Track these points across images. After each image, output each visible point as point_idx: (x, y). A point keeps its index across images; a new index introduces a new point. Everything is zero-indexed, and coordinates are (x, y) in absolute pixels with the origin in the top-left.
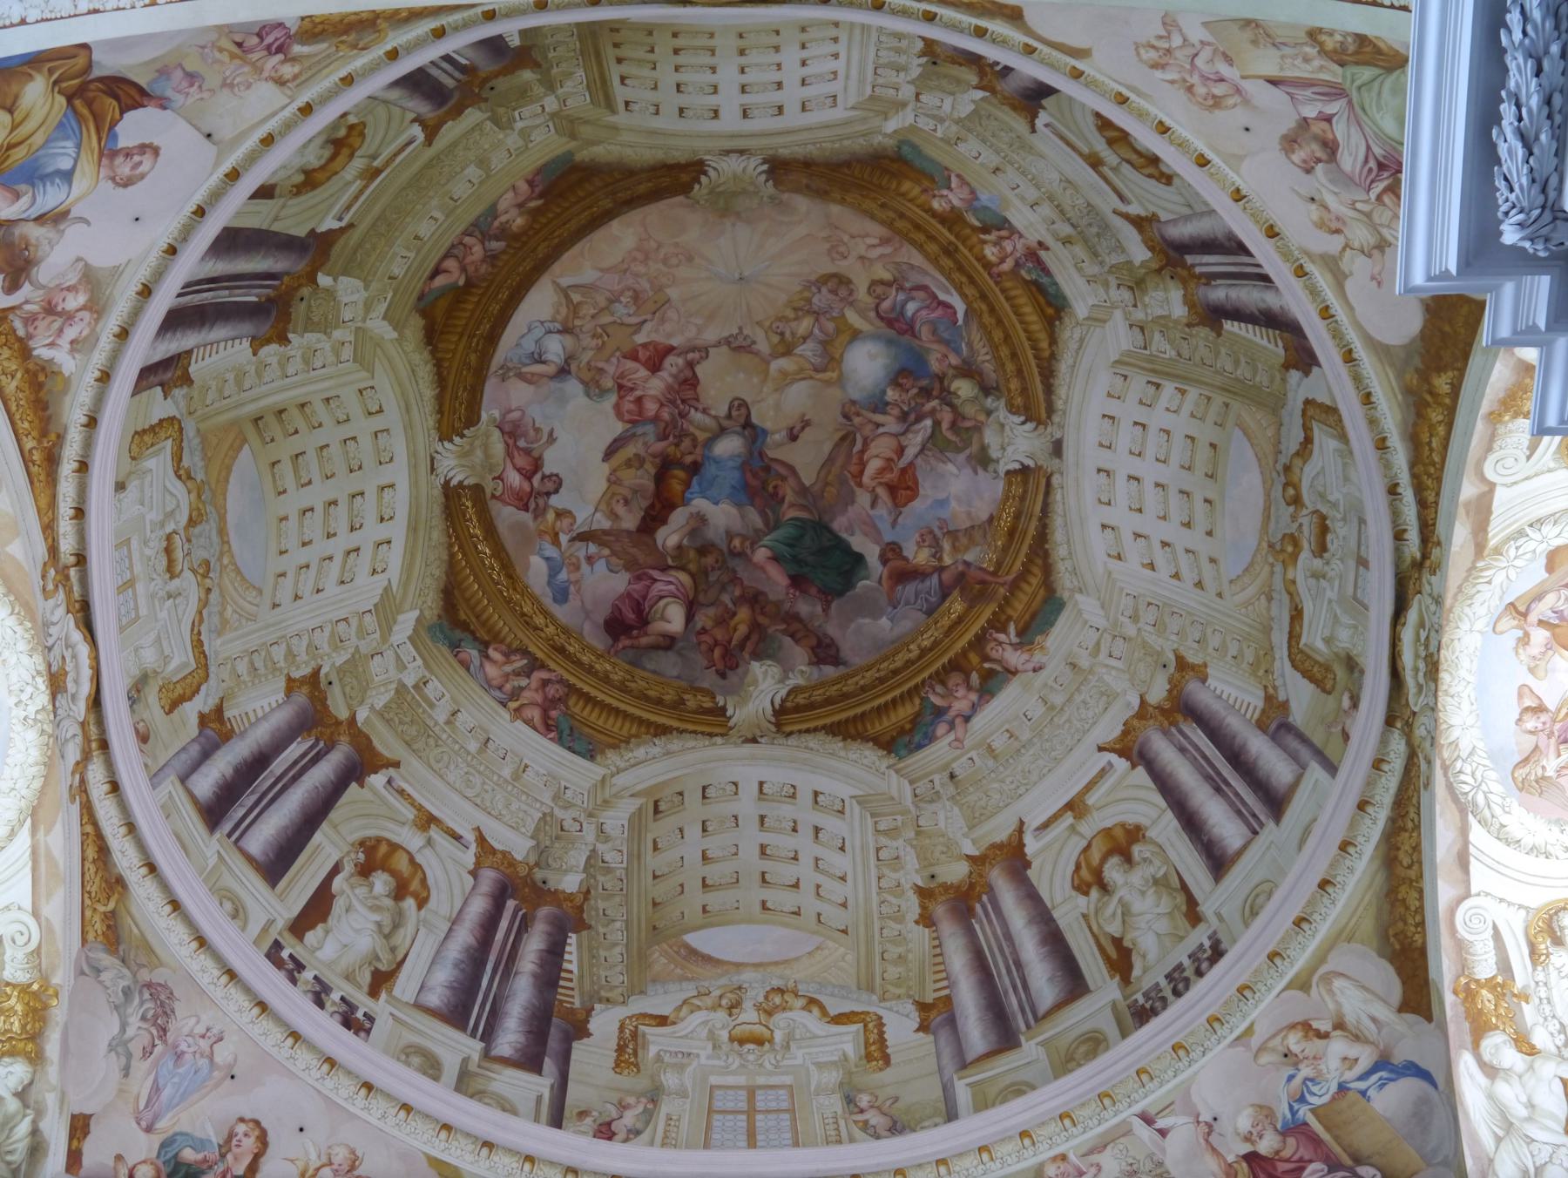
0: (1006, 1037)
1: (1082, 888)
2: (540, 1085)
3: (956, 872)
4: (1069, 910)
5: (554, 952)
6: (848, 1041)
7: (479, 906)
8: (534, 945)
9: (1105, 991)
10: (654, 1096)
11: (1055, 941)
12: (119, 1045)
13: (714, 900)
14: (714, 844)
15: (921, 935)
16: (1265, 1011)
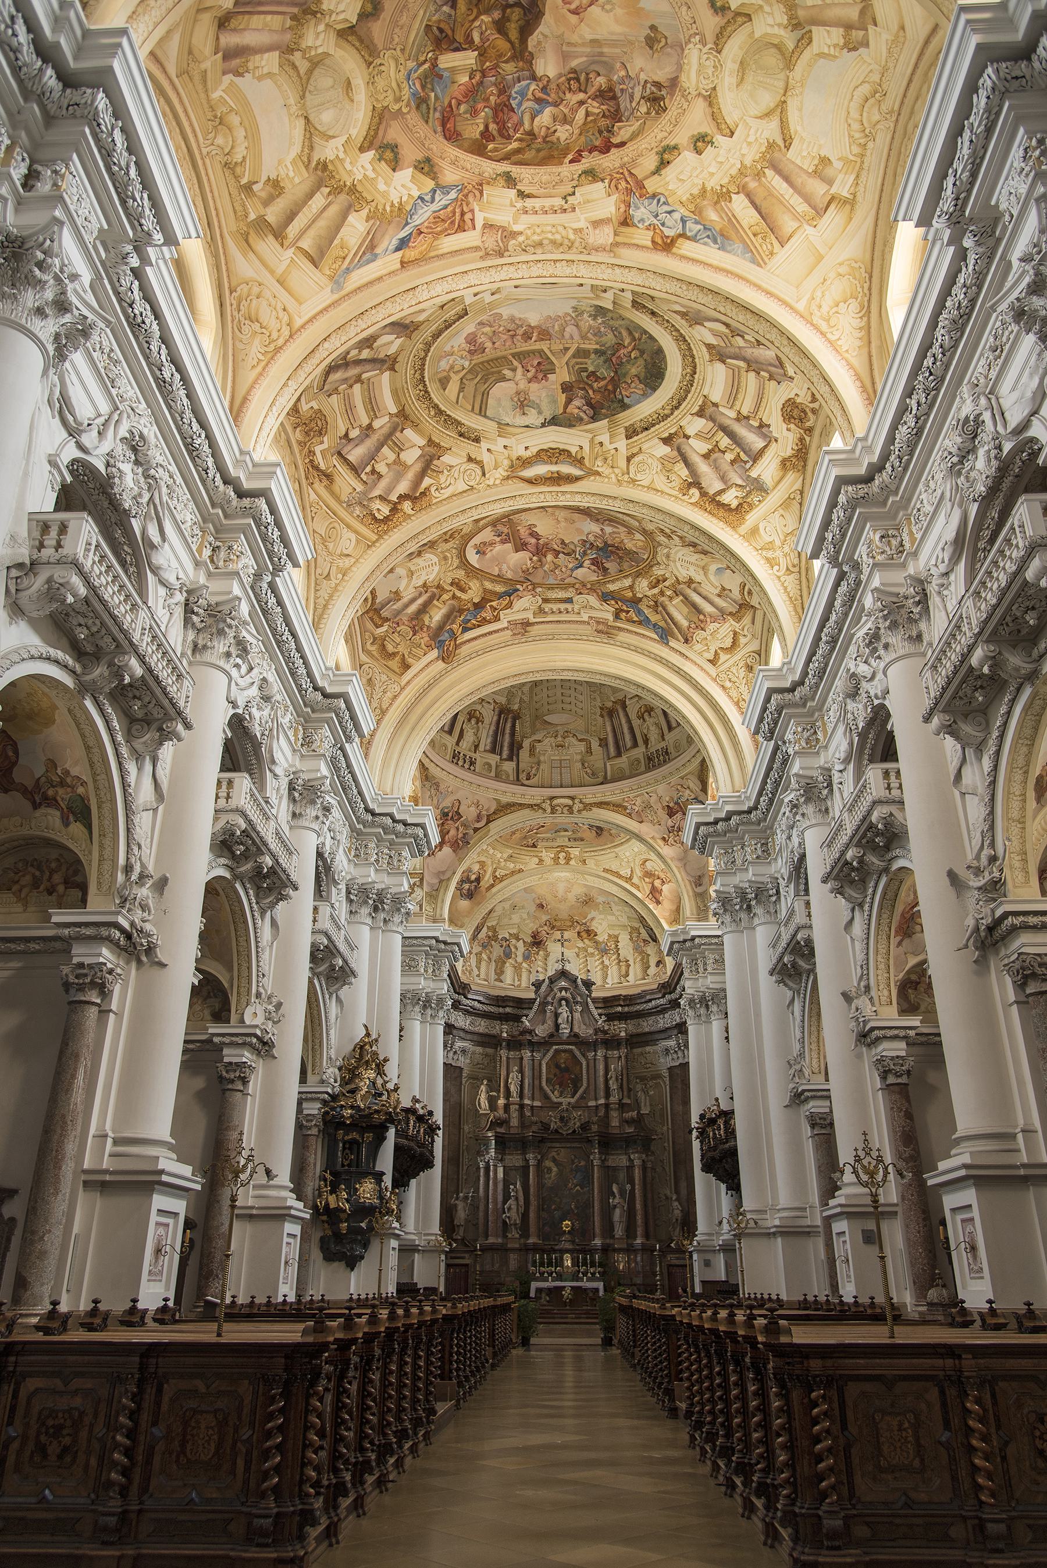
0: (619, 754)
1: (639, 718)
2: (513, 764)
3: (609, 705)
4: (636, 722)
5: (513, 726)
6: (582, 747)
7: (495, 718)
8: (509, 725)
9: (641, 749)
10: (539, 763)
11: (631, 729)
12: (431, 797)
13: (550, 707)
14: (550, 693)
15: (600, 719)
16: (674, 780)
